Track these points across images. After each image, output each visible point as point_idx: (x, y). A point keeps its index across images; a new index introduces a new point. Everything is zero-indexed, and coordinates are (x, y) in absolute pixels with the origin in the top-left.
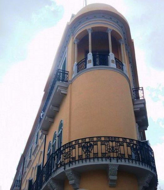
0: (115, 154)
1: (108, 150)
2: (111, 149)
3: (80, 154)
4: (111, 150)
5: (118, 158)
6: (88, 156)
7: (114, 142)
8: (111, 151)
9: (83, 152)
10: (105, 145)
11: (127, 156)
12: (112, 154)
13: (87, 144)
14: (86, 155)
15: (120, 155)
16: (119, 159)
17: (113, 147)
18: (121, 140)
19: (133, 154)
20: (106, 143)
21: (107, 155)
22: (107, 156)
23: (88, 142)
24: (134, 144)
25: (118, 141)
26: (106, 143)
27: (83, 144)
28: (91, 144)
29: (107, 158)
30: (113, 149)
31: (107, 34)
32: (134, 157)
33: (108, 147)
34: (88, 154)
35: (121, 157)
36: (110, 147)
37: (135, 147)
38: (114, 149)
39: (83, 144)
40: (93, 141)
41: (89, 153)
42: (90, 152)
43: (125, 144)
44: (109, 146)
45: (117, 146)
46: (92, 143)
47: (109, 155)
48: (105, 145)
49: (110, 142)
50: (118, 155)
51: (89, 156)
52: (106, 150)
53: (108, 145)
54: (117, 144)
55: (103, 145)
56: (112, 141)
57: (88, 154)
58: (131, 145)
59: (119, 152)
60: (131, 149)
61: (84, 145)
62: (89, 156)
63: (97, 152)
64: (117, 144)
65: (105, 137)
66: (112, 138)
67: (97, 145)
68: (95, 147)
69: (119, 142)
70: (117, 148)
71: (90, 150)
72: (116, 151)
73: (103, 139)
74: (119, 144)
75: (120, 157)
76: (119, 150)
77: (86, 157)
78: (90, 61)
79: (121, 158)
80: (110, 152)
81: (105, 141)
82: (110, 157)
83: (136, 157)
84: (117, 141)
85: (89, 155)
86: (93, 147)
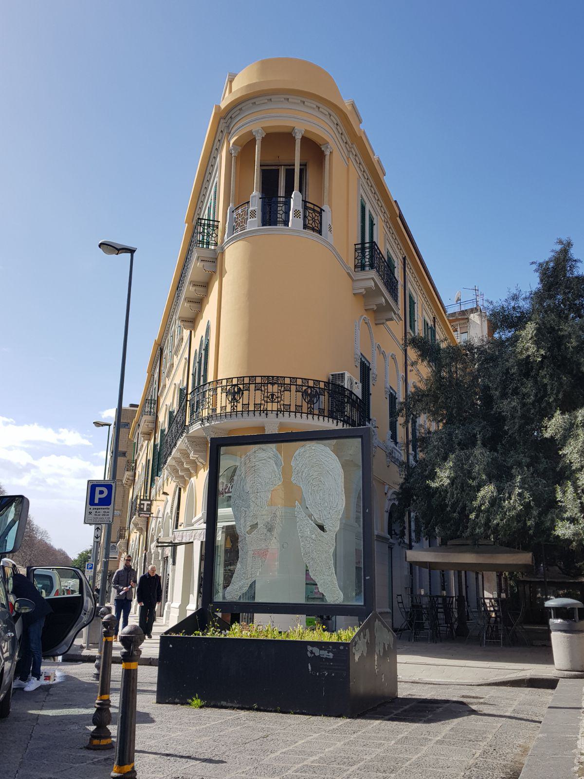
0: (275, 405)
1: (265, 399)
2: (269, 397)
3: (223, 405)
4: (270, 400)
5: (279, 411)
6: (234, 409)
7: (276, 385)
8: (269, 401)
9: (227, 400)
10: (261, 390)
11: (293, 409)
12: (270, 404)
13: (234, 388)
14: (232, 407)
15: (282, 407)
16: (281, 413)
17: (272, 395)
18: (287, 381)
19: (305, 405)
20: (263, 387)
21: (262, 407)
22: (262, 409)
23: (235, 385)
24: (309, 387)
25: (282, 384)
26: (263, 387)
27: (228, 387)
28: (240, 388)
29: (262, 412)
30: (272, 398)
31: (293, 139)
32: (305, 410)
33: (266, 394)
34: (234, 404)
35: (285, 409)
36: (269, 394)
37: (309, 391)
38: (275, 397)
39: (228, 387)
40: (243, 384)
41: (235, 403)
42: (237, 402)
43: (293, 388)
44: (268, 392)
45: (279, 391)
46: (241, 386)
47: (265, 407)
48: (261, 390)
49: (269, 385)
50: (279, 407)
51: (235, 408)
52: (262, 398)
53: (266, 391)
54: (280, 388)
55: (257, 390)
56: (273, 384)
57: (234, 404)
58: (304, 388)
59: (282, 402)
60: (302, 395)
61: (229, 389)
62: (235, 408)
63: (247, 403)
64: (280, 388)
65: (261, 376)
66: (273, 379)
67: (249, 390)
68: (246, 393)
69: (284, 384)
70: (279, 395)
71: (238, 399)
72: (276, 401)
73: (258, 380)
74: (283, 389)
75: (282, 410)
76: (282, 399)
77: (231, 410)
78: (253, 214)
79: (284, 411)
80: (267, 402)
81: (261, 383)
82: (267, 411)
83: (308, 408)
84: (281, 384)
85: (236, 406)
86: (243, 394)
